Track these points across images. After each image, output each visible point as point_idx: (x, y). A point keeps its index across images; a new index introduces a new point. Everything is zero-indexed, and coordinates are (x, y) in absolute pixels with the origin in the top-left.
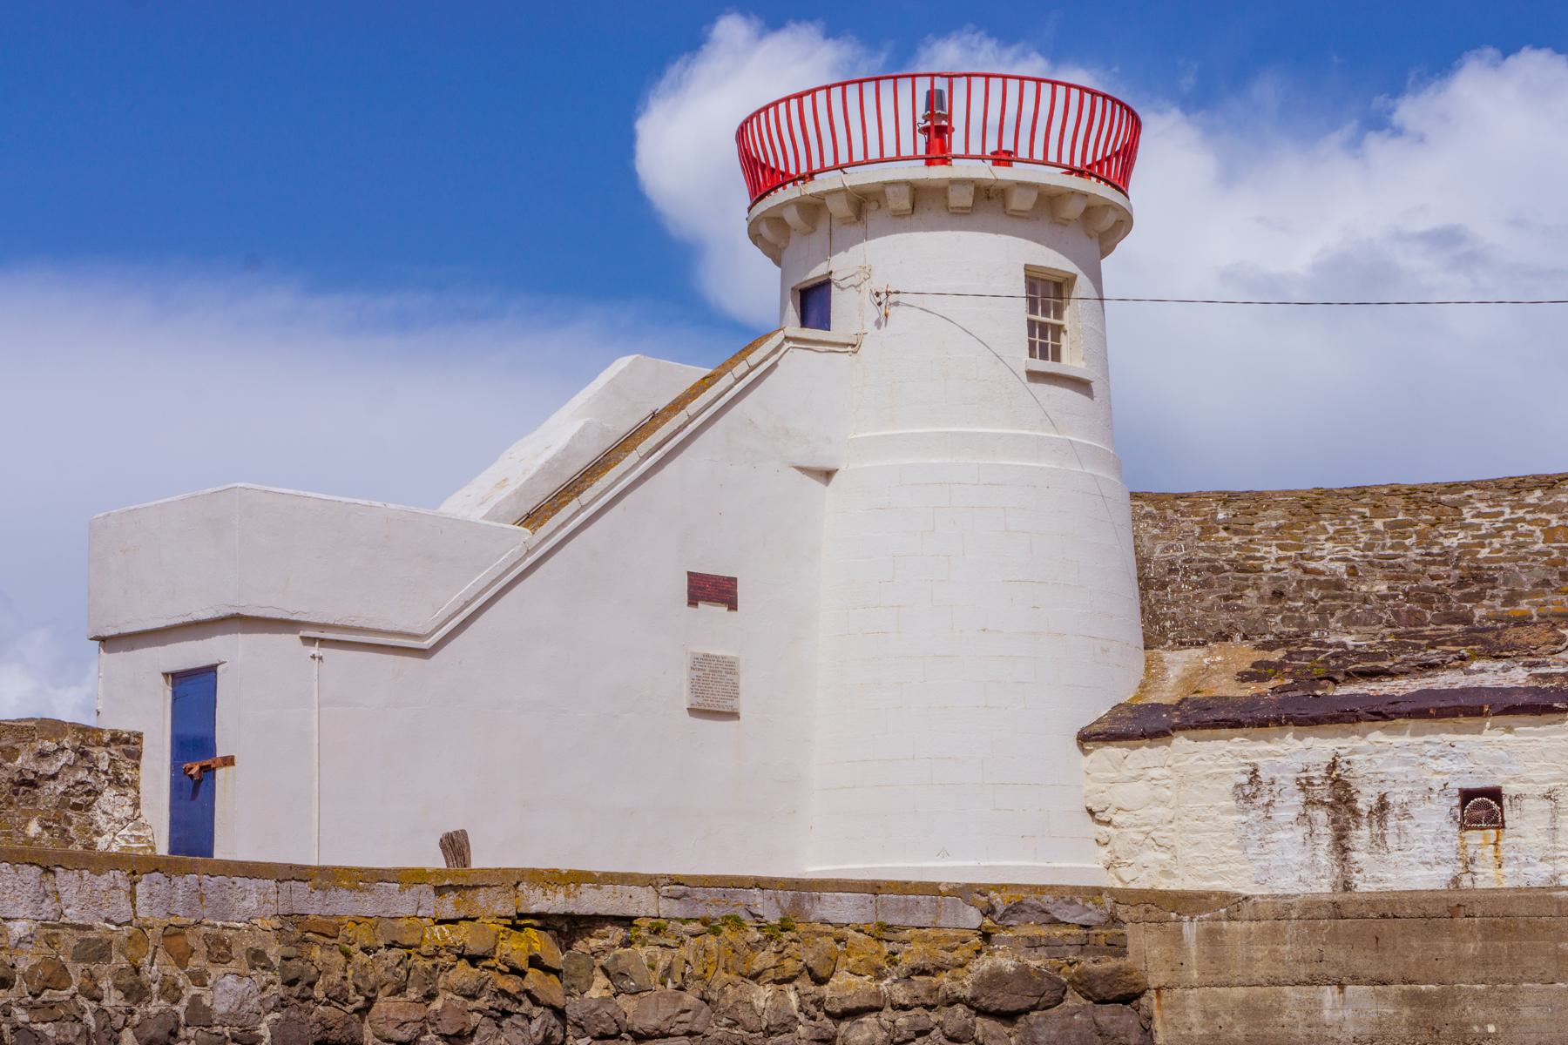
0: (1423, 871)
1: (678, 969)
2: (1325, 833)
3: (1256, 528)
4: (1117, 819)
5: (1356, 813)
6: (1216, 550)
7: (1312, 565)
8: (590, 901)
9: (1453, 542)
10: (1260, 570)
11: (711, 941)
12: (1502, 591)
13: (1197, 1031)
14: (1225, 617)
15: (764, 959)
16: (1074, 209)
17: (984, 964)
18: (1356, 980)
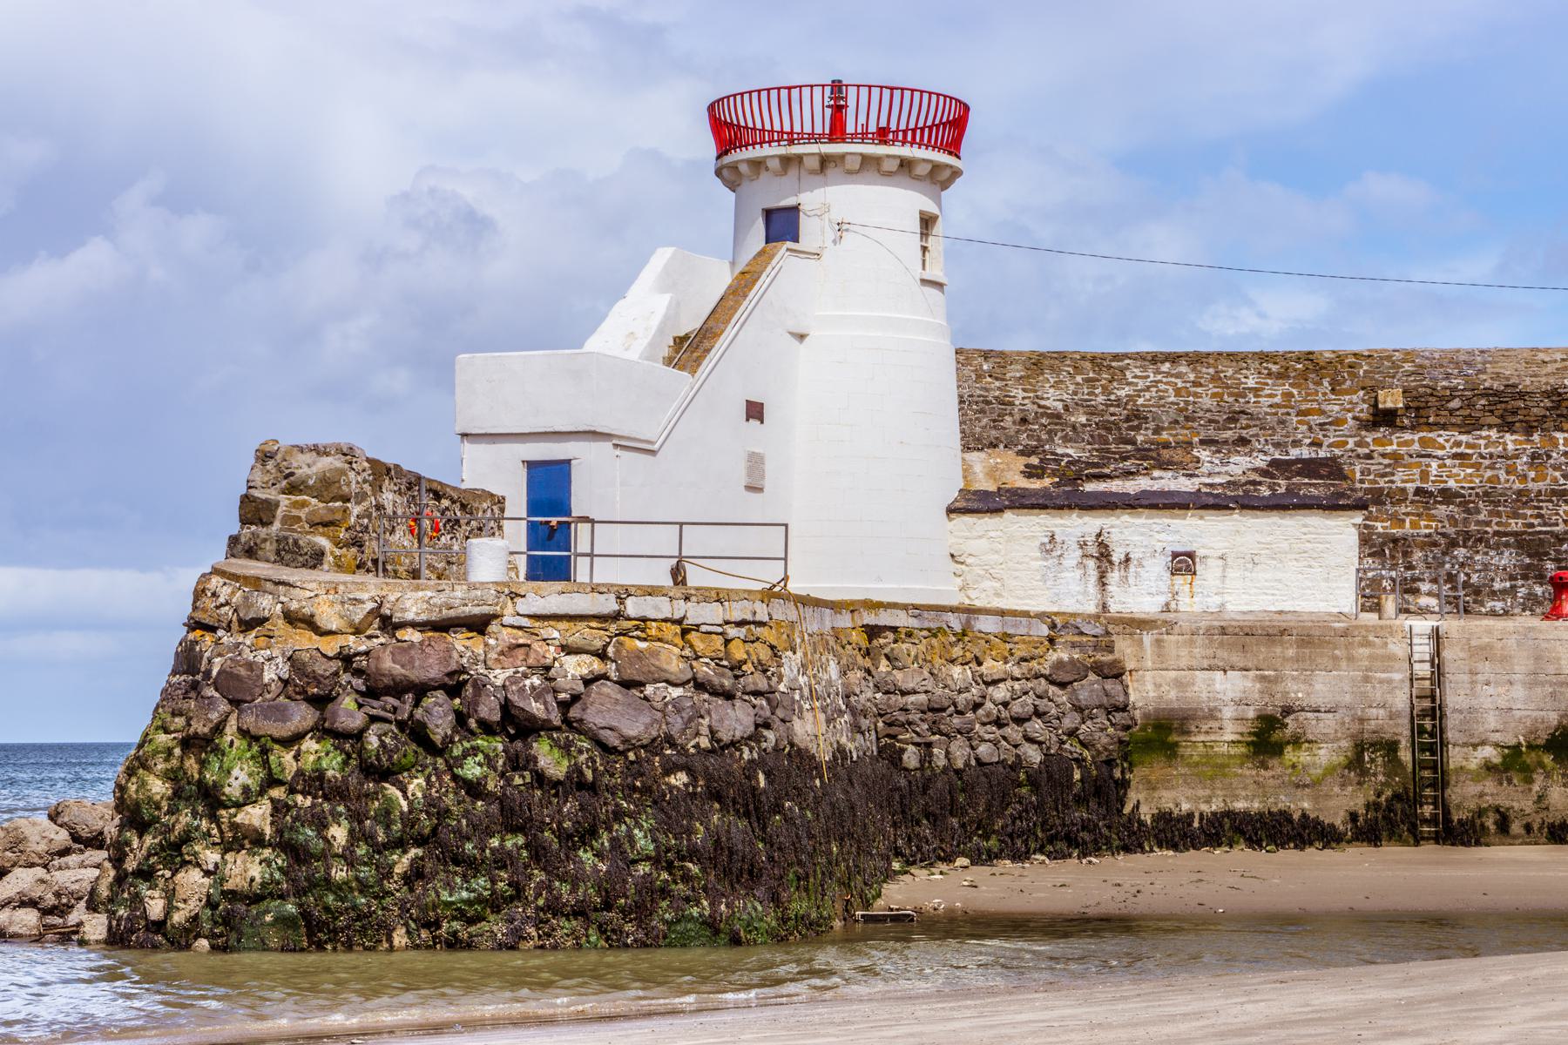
0: (1149, 598)
1: (921, 656)
2: (1093, 574)
3: (1008, 376)
4: (969, 561)
5: (1111, 563)
6: (987, 390)
7: (1042, 403)
8: (884, 618)
9: (1122, 393)
10: (1012, 404)
11: (934, 641)
12: (1152, 425)
13: (1152, 694)
14: (993, 432)
15: (957, 651)
16: (922, 170)
17: (1053, 656)
18: (1233, 668)
